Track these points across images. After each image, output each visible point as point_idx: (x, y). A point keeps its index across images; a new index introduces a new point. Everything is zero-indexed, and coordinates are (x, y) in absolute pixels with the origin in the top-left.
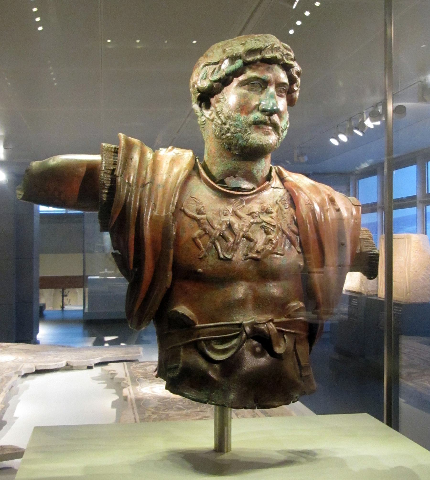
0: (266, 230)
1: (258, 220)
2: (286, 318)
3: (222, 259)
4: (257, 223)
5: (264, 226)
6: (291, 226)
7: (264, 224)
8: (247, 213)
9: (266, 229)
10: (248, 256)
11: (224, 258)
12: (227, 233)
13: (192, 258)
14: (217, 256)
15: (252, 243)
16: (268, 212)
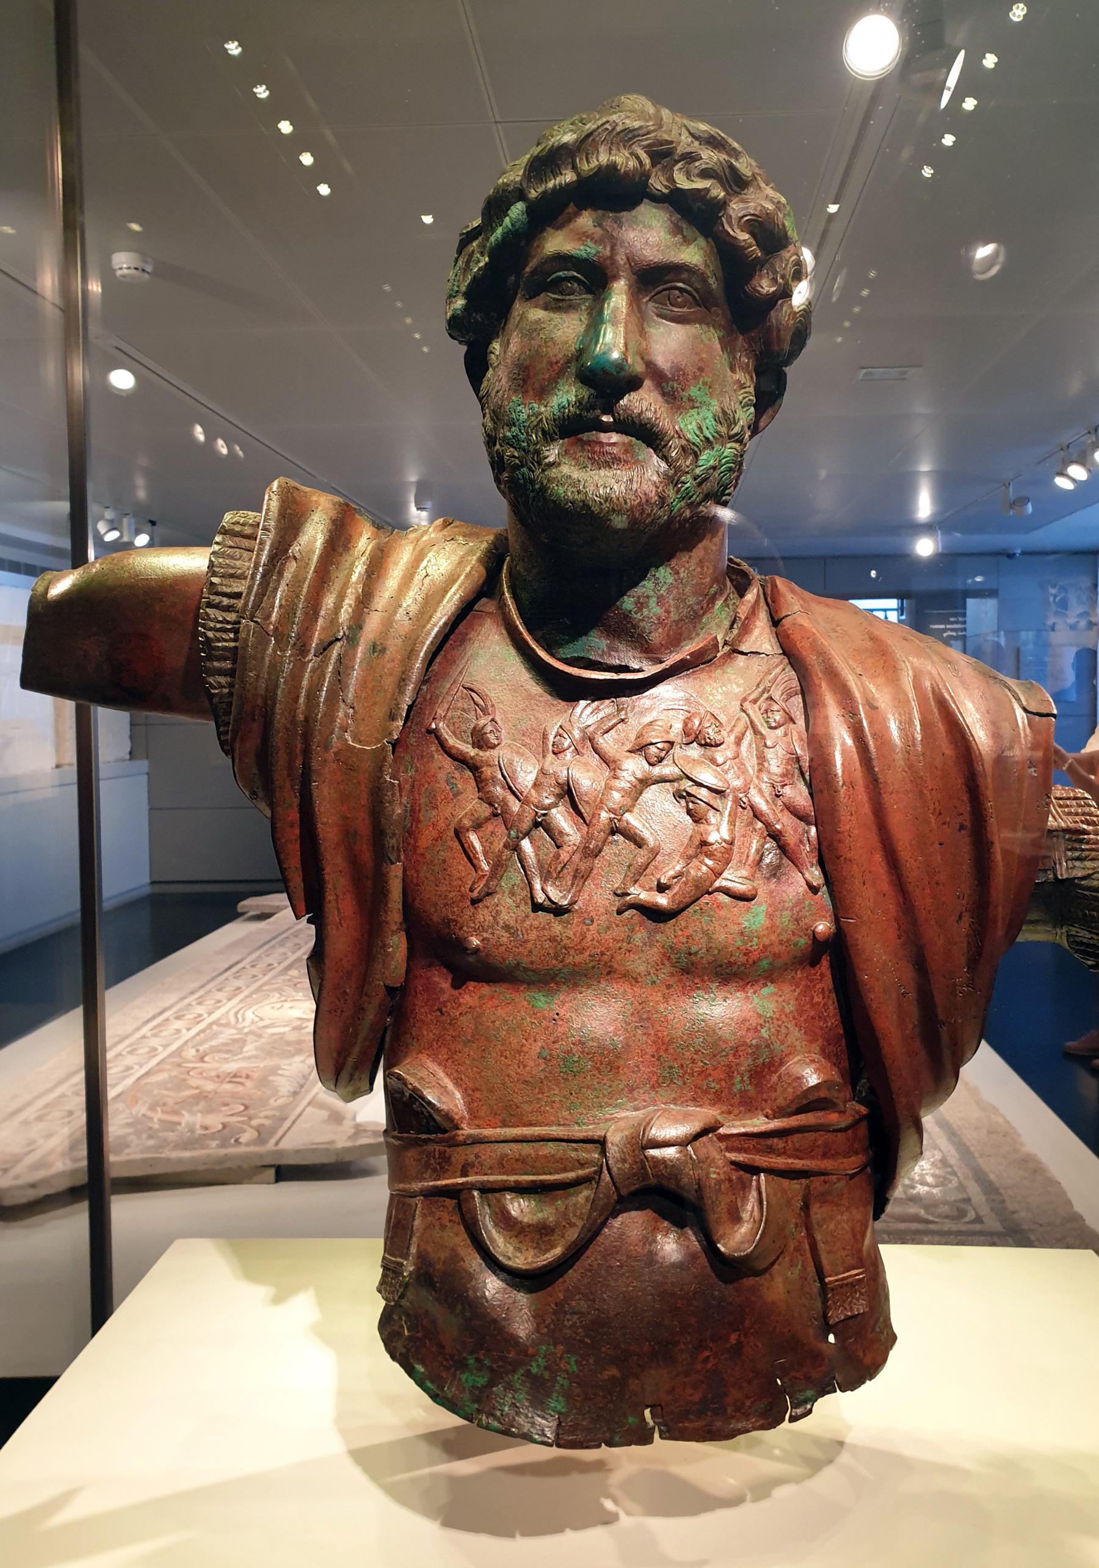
0: (691, 805)
1: (667, 769)
2: (767, 1117)
3: (537, 907)
4: (663, 780)
5: (685, 794)
6: (787, 791)
7: (687, 785)
8: (628, 746)
9: (693, 802)
10: (628, 898)
11: (547, 903)
12: (561, 817)
13: (452, 894)
14: (525, 893)
15: (642, 852)
16: (703, 742)
